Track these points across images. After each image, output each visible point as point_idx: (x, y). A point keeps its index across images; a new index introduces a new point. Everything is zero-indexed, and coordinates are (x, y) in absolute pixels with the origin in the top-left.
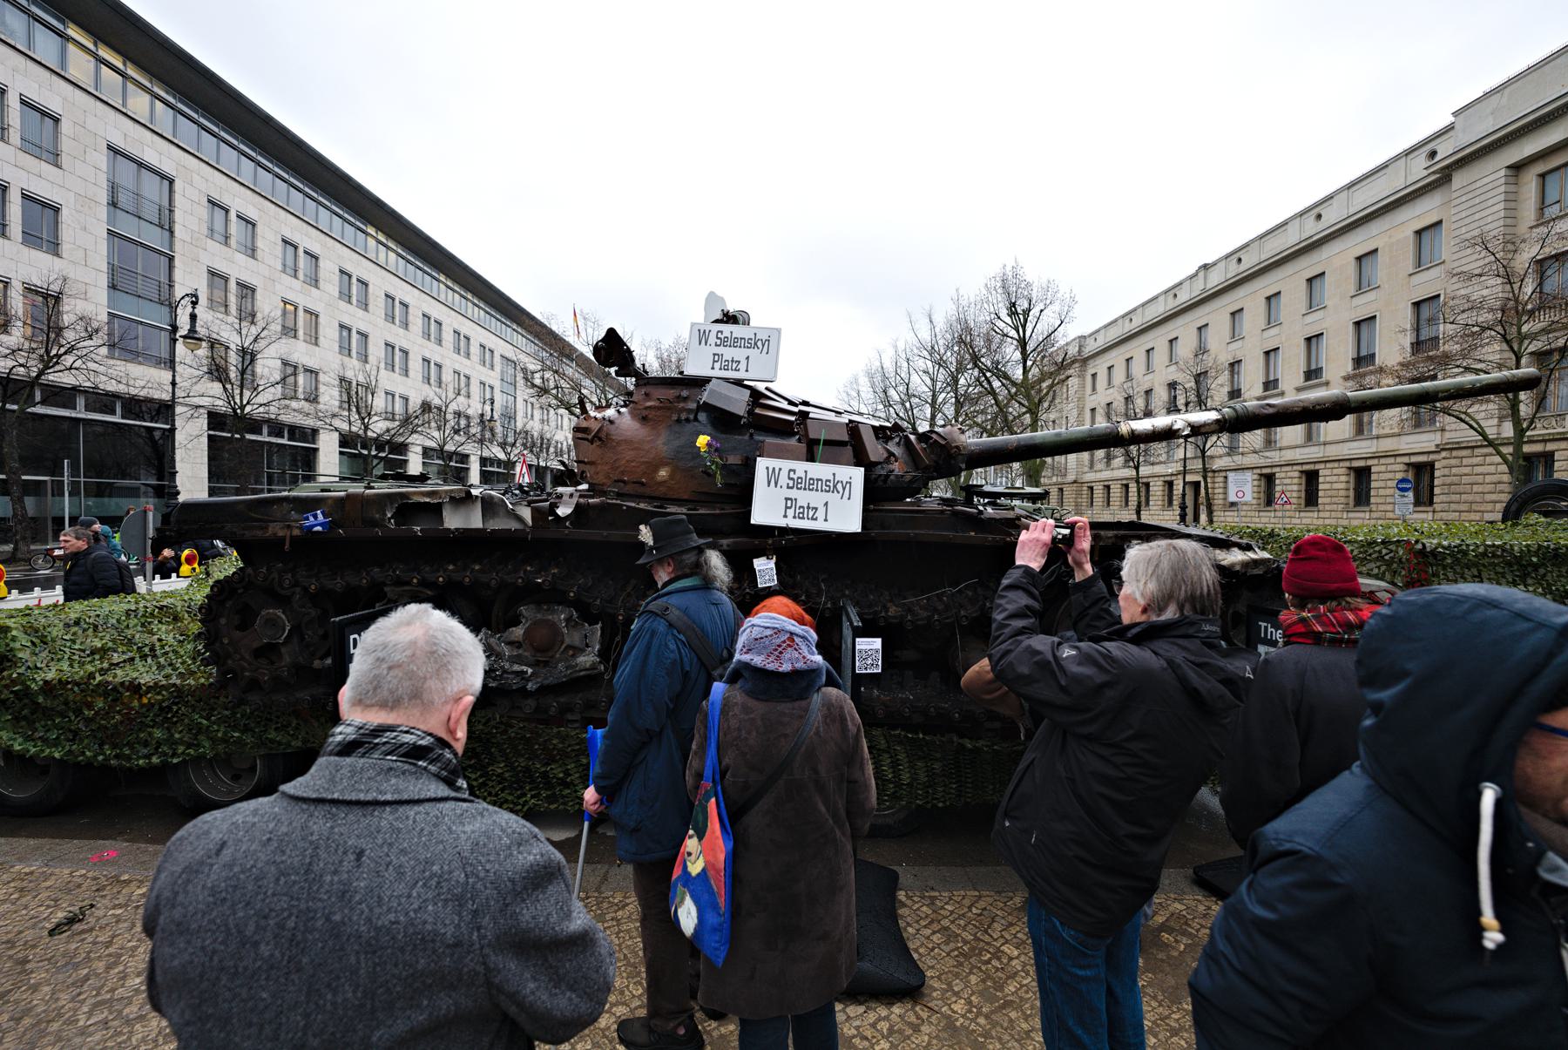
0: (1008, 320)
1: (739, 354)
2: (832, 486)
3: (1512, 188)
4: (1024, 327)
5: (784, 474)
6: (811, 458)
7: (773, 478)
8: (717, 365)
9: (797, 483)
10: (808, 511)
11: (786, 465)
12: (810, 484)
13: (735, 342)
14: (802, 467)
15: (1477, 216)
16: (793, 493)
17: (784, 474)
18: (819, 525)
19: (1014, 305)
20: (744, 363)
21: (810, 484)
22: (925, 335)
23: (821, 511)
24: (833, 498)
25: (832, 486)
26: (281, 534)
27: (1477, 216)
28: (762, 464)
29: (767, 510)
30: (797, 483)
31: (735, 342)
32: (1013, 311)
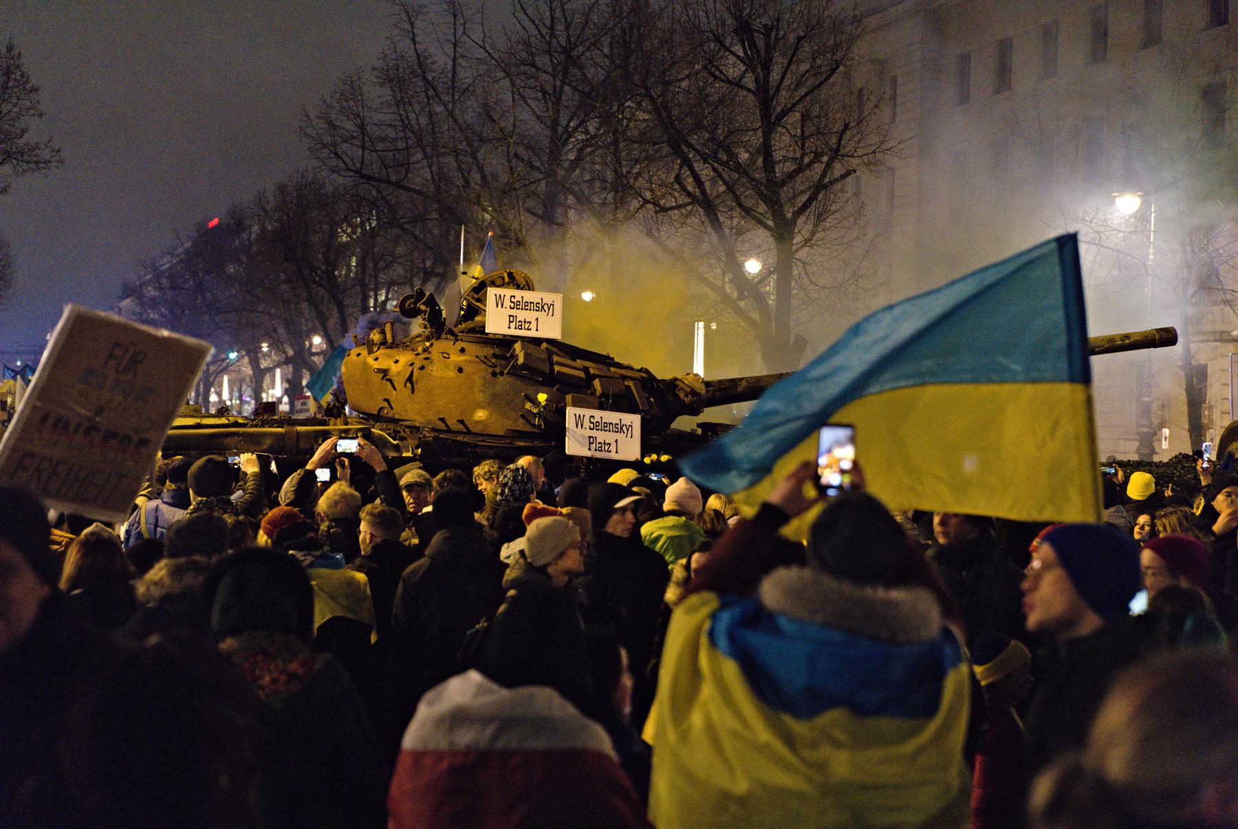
1: (529, 315)
2: (619, 428)
7: (579, 421)
8: (513, 325)
9: (596, 426)
11: (587, 412)
12: (606, 427)
13: (526, 306)
14: (598, 414)
16: (594, 433)
18: (613, 456)
20: (534, 323)
21: (606, 427)
24: (620, 436)
25: (619, 428)
28: (571, 412)
29: (574, 446)
30: (596, 426)
31: (526, 306)
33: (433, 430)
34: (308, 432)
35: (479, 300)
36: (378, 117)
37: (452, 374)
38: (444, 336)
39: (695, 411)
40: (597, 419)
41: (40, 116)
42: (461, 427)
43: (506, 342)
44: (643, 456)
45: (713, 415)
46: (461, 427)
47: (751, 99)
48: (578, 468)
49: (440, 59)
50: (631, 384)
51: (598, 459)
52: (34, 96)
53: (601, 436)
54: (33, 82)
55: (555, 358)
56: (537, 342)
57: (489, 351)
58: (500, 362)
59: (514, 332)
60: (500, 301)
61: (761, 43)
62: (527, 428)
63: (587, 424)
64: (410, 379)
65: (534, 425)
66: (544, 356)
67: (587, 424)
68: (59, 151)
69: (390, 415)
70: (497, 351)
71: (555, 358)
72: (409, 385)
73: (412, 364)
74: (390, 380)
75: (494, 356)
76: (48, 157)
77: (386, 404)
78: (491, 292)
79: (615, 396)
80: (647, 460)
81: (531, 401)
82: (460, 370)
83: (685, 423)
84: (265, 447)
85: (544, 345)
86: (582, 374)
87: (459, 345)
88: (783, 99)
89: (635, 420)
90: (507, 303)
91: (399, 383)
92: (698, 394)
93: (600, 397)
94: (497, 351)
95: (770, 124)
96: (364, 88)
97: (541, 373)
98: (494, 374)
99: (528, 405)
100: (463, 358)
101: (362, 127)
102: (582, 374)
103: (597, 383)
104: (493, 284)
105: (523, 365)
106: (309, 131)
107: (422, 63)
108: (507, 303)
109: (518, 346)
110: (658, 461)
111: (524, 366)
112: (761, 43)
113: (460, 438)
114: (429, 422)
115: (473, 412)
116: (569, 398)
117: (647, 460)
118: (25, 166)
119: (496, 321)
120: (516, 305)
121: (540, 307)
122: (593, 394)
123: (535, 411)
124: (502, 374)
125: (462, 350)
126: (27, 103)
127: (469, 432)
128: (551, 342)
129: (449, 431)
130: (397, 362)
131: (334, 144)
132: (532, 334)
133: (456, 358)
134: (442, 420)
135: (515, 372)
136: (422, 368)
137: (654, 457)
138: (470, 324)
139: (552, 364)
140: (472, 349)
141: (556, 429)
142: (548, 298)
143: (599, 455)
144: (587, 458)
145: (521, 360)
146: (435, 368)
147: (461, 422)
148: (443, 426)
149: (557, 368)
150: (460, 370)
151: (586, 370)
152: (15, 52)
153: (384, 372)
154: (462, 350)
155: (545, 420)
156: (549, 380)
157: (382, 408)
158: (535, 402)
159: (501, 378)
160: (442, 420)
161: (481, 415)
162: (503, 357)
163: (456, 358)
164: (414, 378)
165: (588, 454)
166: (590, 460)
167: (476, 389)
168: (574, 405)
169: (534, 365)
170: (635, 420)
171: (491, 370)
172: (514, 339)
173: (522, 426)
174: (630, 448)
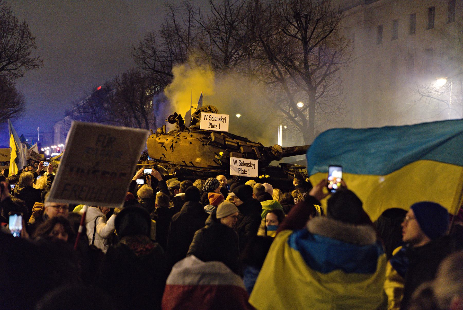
2: (250, 165)
5: (238, 162)
7: (235, 162)
8: (210, 126)
9: (241, 164)
11: (238, 159)
12: (245, 165)
13: (215, 119)
14: (242, 160)
16: (241, 167)
17: (238, 162)
20: (218, 126)
21: (245, 165)
25: (250, 165)
28: (232, 159)
30: (241, 164)
31: (215, 119)
33: (181, 165)
35: (198, 117)
36: (160, 49)
37: (188, 144)
38: (185, 130)
39: (278, 159)
40: (242, 161)
41: (35, 48)
42: (190, 164)
43: (208, 133)
44: (259, 176)
45: (284, 160)
46: (190, 164)
47: (300, 42)
49: (184, 27)
50: (254, 148)
51: (242, 177)
52: (33, 41)
53: (243, 168)
54: (33, 36)
55: (226, 139)
56: (219, 133)
57: (201, 136)
58: (205, 140)
59: (211, 129)
60: (205, 117)
61: (304, 21)
62: (216, 165)
63: (238, 163)
64: (172, 146)
65: (218, 164)
66: (222, 138)
67: (238, 163)
68: (42, 61)
69: (165, 160)
70: (204, 136)
72: (171, 149)
73: (173, 141)
74: (164, 147)
75: (203, 138)
76: (38, 64)
77: (163, 156)
78: (202, 114)
79: (248, 153)
80: (260, 177)
81: (217, 155)
82: (191, 143)
83: (275, 163)
85: (222, 134)
86: (236, 145)
87: (190, 134)
88: (312, 42)
89: (256, 162)
90: (208, 118)
91: (168, 148)
92: (280, 153)
93: (243, 153)
94: (204, 136)
96: (155, 38)
97: (221, 144)
98: (203, 145)
99: (216, 156)
100: (192, 139)
101: (154, 52)
102: (236, 145)
103: (242, 148)
104: (203, 111)
105: (214, 141)
106: (135, 54)
107: (177, 28)
108: (208, 118)
109: (212, 134)
110: (265, 177)
111: (214, 142)
112: (304, 21)
113: (190, 169)
114: (179, 162)
115: (195, 159)
116: (231, 154)
118: (30, 67)
119: (204, 125)
120: (212, 119)
121: (221, 120)
122: (240, 152)
123: (219, 158)
124: (206, 144)
125: (192, 136)
126: (31, 44)
127: (194, 166)
128: (224, 132)
129: (186, 166)
130: (167, 140)
131: (144, 59)
133: (189, 139)
134: (184, 162)
135: (211, 144)
136: (176, 142)
137: (263, 176)
138: (194, 126)
139: (225, 141)
142: (224, 116)
143: (242, 175)
145: (213, 140)
147: (191, 162)
148: (184, 164)
149: (227, 142)
150: (191, 143)
151: (237, 143)
152: (26, 24)
153: (162, 144)
154: (192, 136)
155: (222, 162)
156: (224, 147)
157: (161, 157)
158: (219, 155)
159: (206, 146)
160: (184, 162)
161: (198, 160)
162: (207, 138)
163: (189, 139)
165: (238, 175)
167: (197, 150)
168: (233, 156)
169: (218, 141)
170: (256, 162)
172: (211, 132)
173: (214, 164)
174: (254, 173)
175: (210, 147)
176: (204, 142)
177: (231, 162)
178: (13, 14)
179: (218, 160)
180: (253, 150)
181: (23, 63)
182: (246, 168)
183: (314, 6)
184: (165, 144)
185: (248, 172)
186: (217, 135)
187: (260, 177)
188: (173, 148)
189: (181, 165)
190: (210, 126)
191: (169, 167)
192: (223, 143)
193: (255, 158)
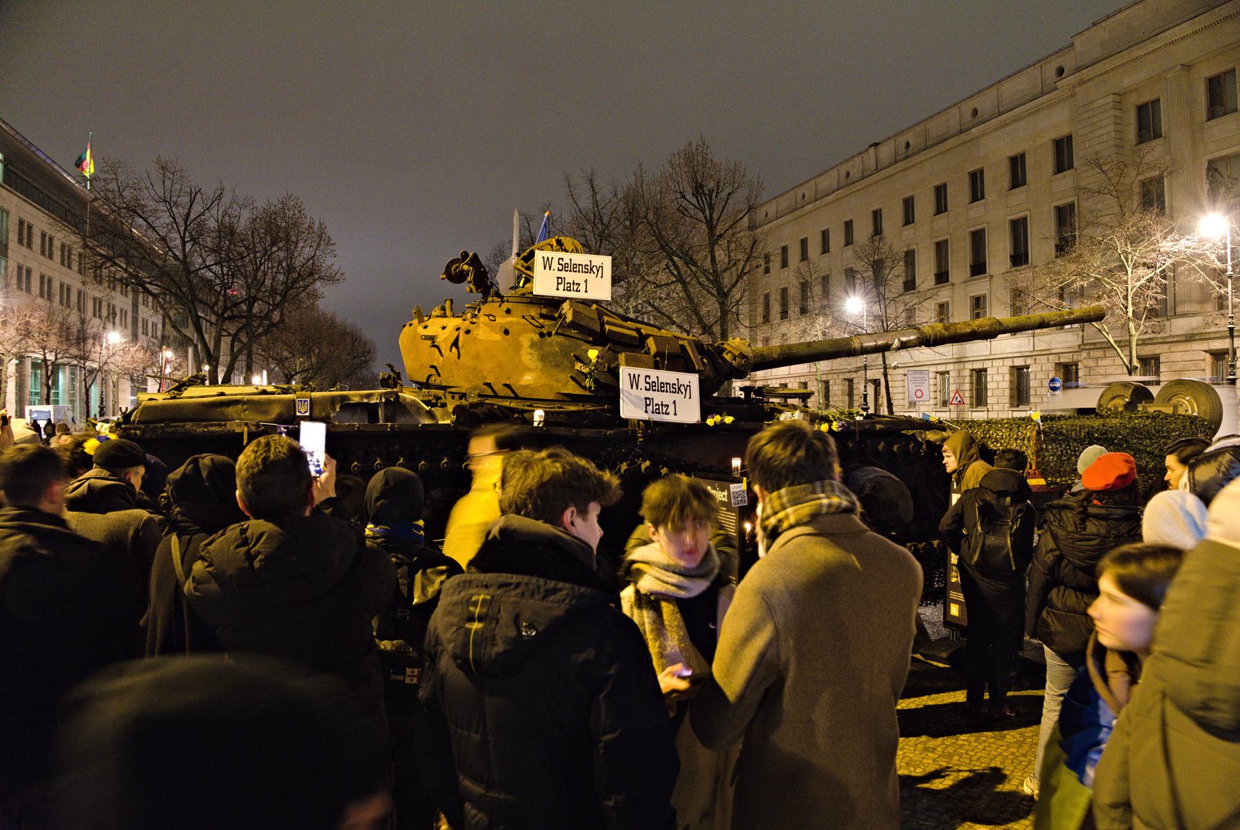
0: (694, 200)
2: (677, 389)
3: (1117, 113)
4: (711, 208)
5: (642, 379)
6: (657, 367)
7: (634, 381)
8: (561, 287)
9: (652, 386)
10: (661, 408)
11: (642, 372)
12: (662, 387)
14: (654, 374)
15: (1096, 134)
16: (650, 394)
17: (642, 379)
18: (670, 418)
19: (701, 186)
21: (662, 387)
22: (586, 203)
23: (671, 410)
24: (678, 397)
25: (677, 389)
26: (238, 430)
27: (1096, 134)
28: (625, 372)
29: (630, 410)
30: (652, 386)
32: (698, 189)
33: (480, 395)
34: (324, 398)
37: (498, 337)
38: (490, 299)
39: (741, 375)
40: (653, 379)
43: (553, 303)
44: (704, 416)
45: (762, 377)
47: (704, 227)
48: (635, 432)
50: (686, 343)
51: (657, 424)
52: (333, 248)
53: (658, 397)
55: (606, 318)
56: (587, 303)
57: (534, 311)
58: (547, 322)
59: (562, 293)
60: (547, 263)
63: (642, 384)
64: (455, 343)
65: (584, 388)
66: (596, 317)
67: (642, 384)
69: (438, 382)
70: (544, 311)
71: (606, 318)
72: (454, 349)
73: (458, 329)
75: (542, 316)
79: (671, 356)
82: (506, 332)
83: (737, 387)
84: (273, 416)
85: (594, 306)
86: (634, 334)
87: (505, 306)
88: (718, 231)
89: (693, 380)
90: (555, 265)
91: (445, 348)
92: (746, 357)
93: (655, 356)
94: (544, 311)
95: (713, 242)
97: (590, 332)
98: (542, 335)
99: (578, 366)
100: (509, 319)
102: (634, 334)
103: (651, 342)
105: (572, 322)
108: (555, 265)
109: (566, 306)
111: (573, 325)
113: (506, 404)
114: (475, 388)
115: (522, 375)
116: (622, 357)
117: (710, 422)
119: (544, 284)
120: (564, 267)
122: (648, 353)
123: (586, 370)
124: (550, 334)
125: (508, 311)
127: (516, 397)
129: (496, 396)
130: (444, 328)
132: (581, 295)
133: (503, 320)
134: (489, 385)
135: (566, 329)
136: (468, 332)
137: (718, 418)
139: (602, 325)
140: (519, 309)
141: (609, 392)
142: (597, 260)
143: (656, 417)
144: (644, 421)
145: (569, 318)
146: (481, 331)
148: (489, 392)
149: (607, 327)
151: (638, 330)
154: (508, 311)
155: (596, 381)
156: (599, 339)
157: (429, 376)
159: (548, 339)
161: (528, 379)
162: (552, 318)
163: (503, 320)
164: (460, 343)
165: (645, 417)
166: (647, 423)
168: (628, 364)
170: (693, 380)
171: (538, 330)
172: (564, 300)
173: (572, 388)
175: (560, 339)
176: (542, 327)
177: (624, 383)
178: (305, 212)
179: (585, 375)
180: (683, 347)
181: (321, 278)
182: (667, 398)
183: (723, 173)
184: (438, 341)
185: (671, 410)
186: (581, 307)
187: (710, 422)
188: (457, 347)
189: (480, 395)
190: (561, 287)
191: (443, 401)
192: (598, 328)
193: (689, 369)
